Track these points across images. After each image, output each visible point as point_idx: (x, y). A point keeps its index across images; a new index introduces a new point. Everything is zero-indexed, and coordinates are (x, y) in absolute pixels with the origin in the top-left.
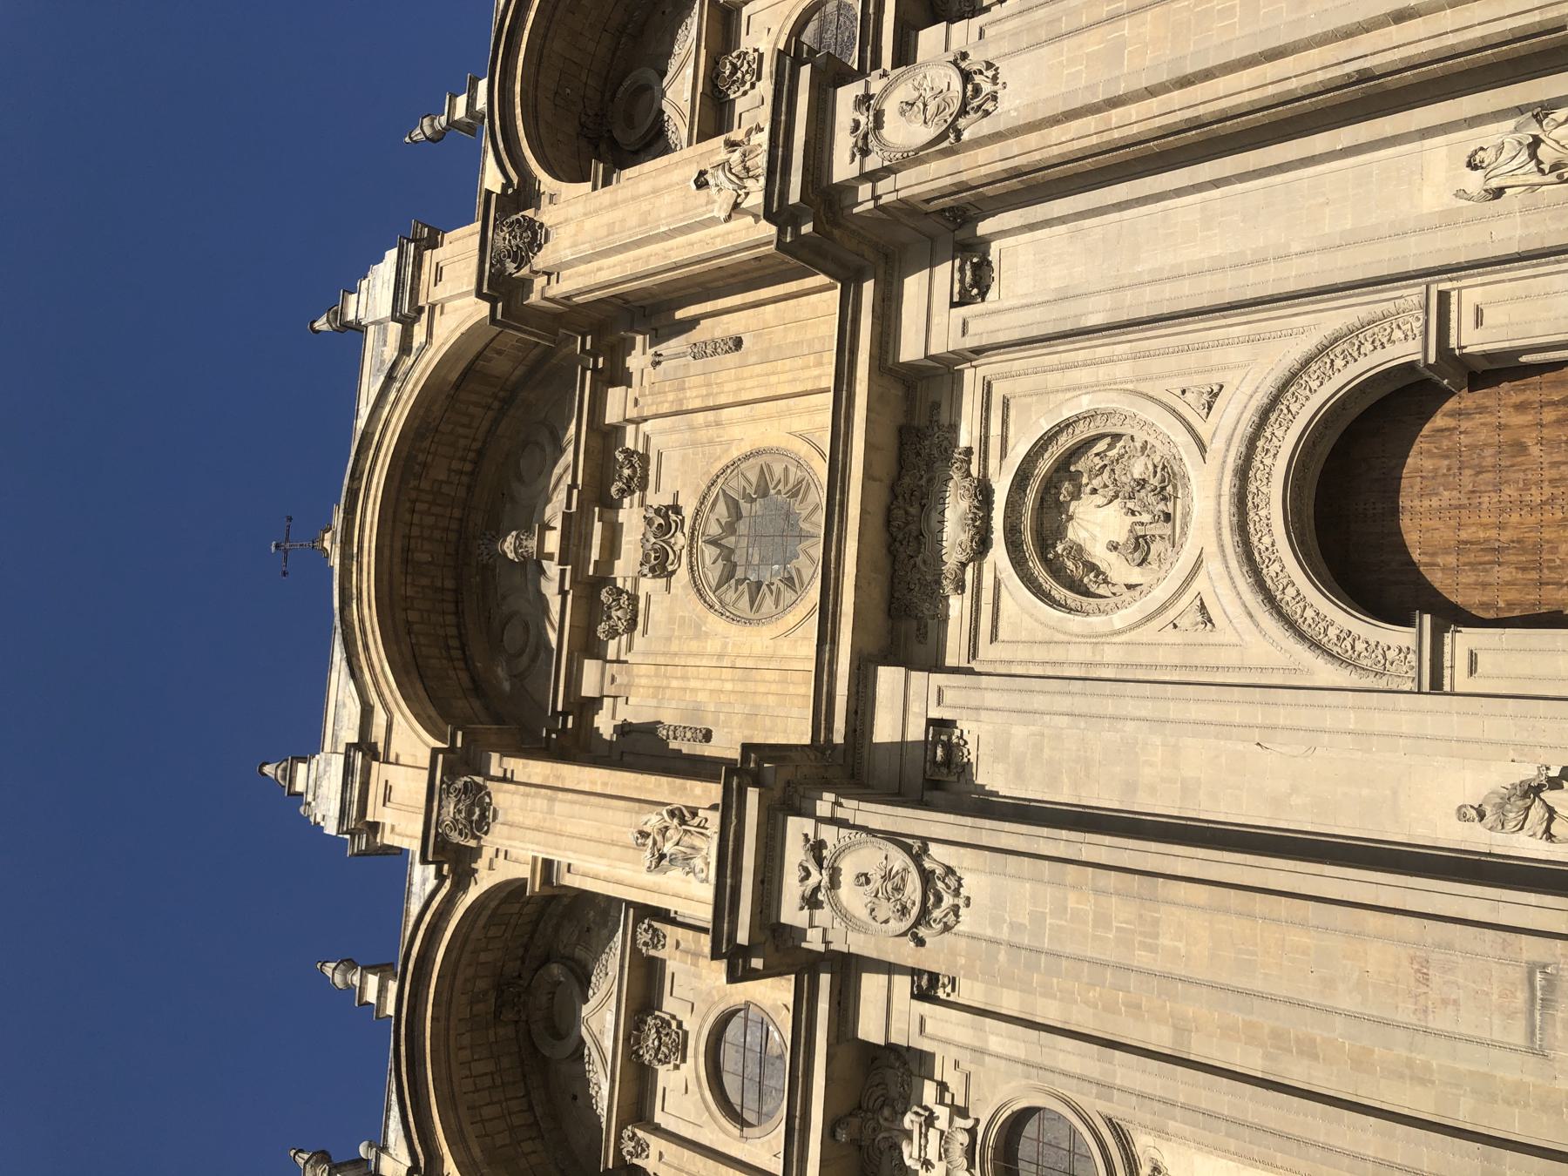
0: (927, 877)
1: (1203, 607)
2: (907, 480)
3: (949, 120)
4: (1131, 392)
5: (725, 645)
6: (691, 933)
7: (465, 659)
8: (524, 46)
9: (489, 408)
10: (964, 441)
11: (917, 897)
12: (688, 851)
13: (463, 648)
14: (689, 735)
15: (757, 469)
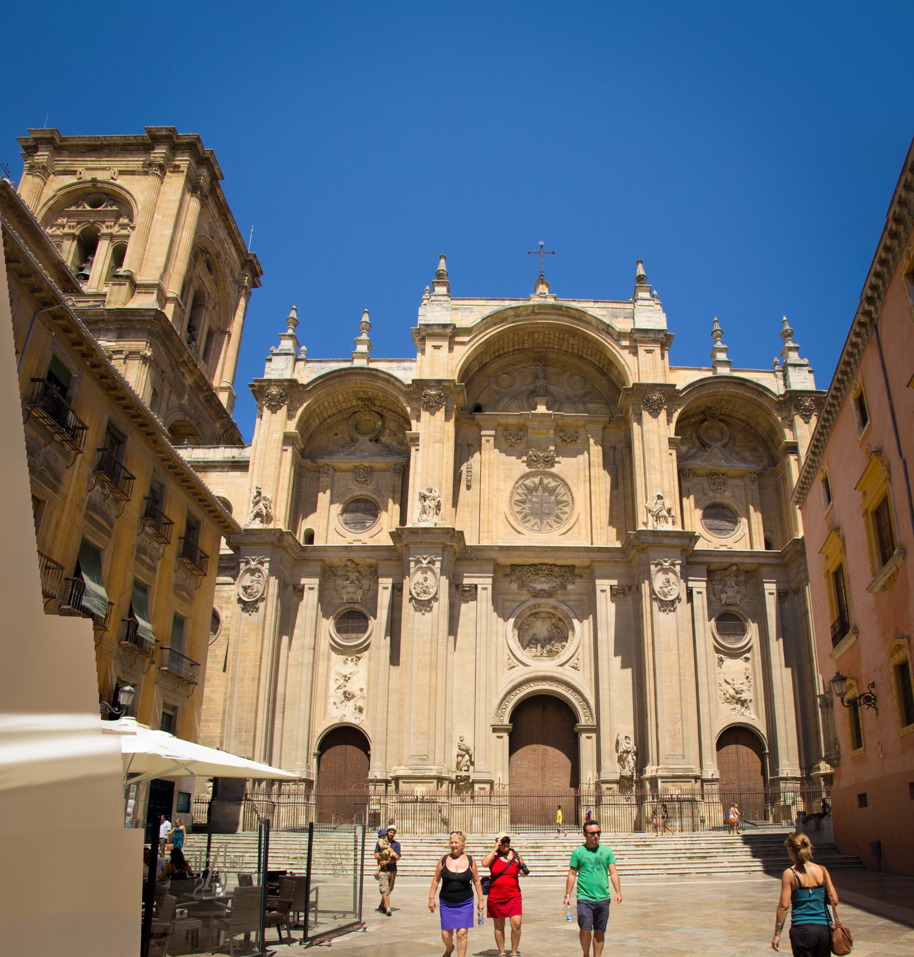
0: (429, 601)
1: (513, 667)
2: (556, 569)
3: (660, 596)
4: (579, 644)
5: (502, 491)
6: (400, 488)
7: (495, 358)
8: (738, 391)
9: (599, 363)
10: (570, 587)
11: (423, 598)
12: (427, 511)
13: (500, 356)
14: (469, 478)
15: (567, 499)
